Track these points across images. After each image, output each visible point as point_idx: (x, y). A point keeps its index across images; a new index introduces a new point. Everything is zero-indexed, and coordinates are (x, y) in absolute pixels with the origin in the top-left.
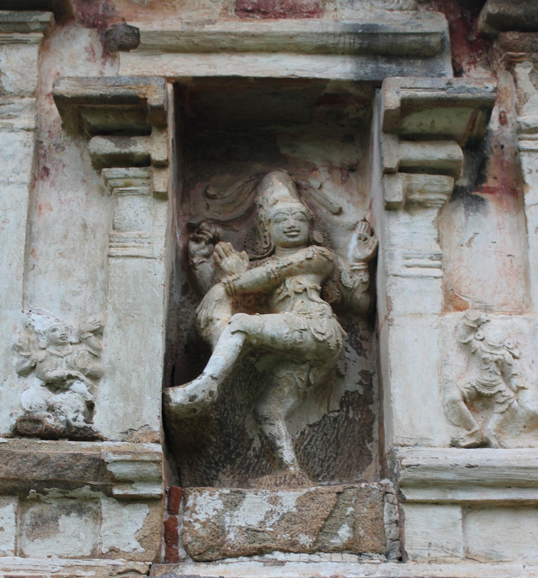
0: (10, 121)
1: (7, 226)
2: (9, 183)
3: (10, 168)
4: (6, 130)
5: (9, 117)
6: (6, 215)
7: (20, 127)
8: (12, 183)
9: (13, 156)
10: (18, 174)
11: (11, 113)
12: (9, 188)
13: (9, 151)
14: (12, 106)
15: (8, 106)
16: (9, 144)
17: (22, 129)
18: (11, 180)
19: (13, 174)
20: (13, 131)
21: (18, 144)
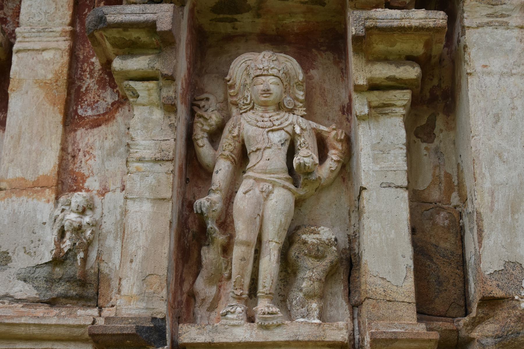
0: (505, 19)
1: (516, 112)
2: (512, 75)
3: (511, 61)
4: (503, 27)
5: (502, 16)
6: (513, 102)
7: (514, 25)
8: (514, 74)
9: (512, 51)
10: (519, 66)
11: (504, 12)
12: (512, 79)
13: (508, 46)
14: (504, 6)
15: (500, 6)
16: (507, 40)
17: (517, 26)
18: (514, 71)
19: (514, 67)
20: (508, 29)
21: (514, 40)
